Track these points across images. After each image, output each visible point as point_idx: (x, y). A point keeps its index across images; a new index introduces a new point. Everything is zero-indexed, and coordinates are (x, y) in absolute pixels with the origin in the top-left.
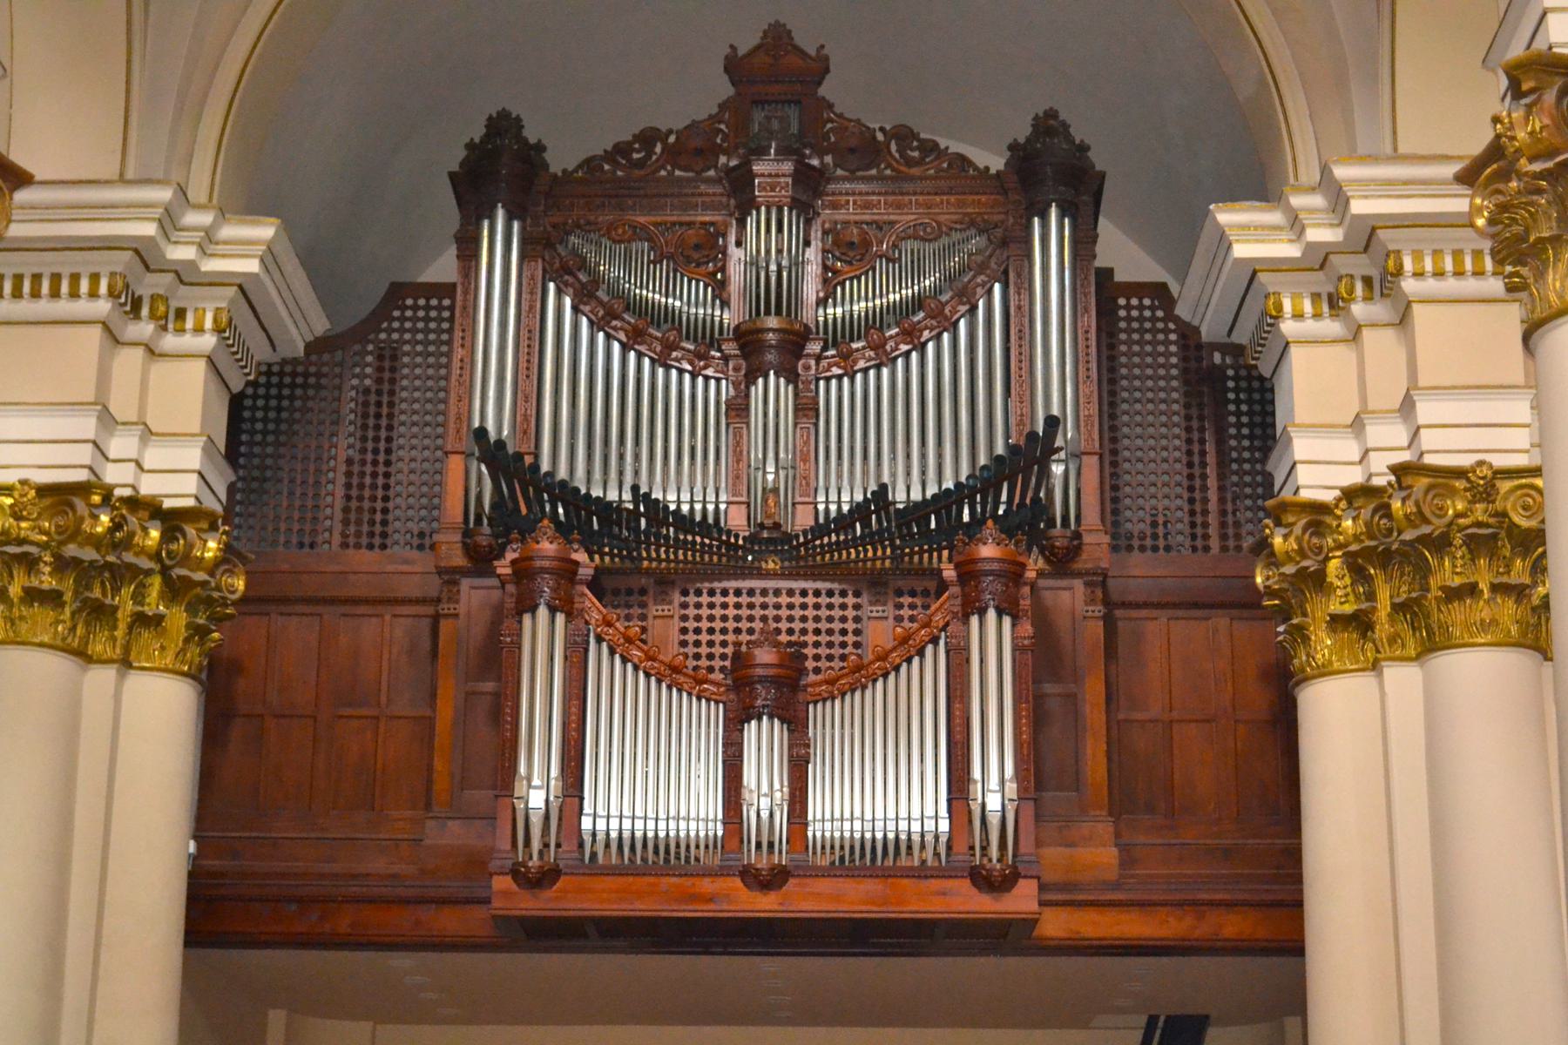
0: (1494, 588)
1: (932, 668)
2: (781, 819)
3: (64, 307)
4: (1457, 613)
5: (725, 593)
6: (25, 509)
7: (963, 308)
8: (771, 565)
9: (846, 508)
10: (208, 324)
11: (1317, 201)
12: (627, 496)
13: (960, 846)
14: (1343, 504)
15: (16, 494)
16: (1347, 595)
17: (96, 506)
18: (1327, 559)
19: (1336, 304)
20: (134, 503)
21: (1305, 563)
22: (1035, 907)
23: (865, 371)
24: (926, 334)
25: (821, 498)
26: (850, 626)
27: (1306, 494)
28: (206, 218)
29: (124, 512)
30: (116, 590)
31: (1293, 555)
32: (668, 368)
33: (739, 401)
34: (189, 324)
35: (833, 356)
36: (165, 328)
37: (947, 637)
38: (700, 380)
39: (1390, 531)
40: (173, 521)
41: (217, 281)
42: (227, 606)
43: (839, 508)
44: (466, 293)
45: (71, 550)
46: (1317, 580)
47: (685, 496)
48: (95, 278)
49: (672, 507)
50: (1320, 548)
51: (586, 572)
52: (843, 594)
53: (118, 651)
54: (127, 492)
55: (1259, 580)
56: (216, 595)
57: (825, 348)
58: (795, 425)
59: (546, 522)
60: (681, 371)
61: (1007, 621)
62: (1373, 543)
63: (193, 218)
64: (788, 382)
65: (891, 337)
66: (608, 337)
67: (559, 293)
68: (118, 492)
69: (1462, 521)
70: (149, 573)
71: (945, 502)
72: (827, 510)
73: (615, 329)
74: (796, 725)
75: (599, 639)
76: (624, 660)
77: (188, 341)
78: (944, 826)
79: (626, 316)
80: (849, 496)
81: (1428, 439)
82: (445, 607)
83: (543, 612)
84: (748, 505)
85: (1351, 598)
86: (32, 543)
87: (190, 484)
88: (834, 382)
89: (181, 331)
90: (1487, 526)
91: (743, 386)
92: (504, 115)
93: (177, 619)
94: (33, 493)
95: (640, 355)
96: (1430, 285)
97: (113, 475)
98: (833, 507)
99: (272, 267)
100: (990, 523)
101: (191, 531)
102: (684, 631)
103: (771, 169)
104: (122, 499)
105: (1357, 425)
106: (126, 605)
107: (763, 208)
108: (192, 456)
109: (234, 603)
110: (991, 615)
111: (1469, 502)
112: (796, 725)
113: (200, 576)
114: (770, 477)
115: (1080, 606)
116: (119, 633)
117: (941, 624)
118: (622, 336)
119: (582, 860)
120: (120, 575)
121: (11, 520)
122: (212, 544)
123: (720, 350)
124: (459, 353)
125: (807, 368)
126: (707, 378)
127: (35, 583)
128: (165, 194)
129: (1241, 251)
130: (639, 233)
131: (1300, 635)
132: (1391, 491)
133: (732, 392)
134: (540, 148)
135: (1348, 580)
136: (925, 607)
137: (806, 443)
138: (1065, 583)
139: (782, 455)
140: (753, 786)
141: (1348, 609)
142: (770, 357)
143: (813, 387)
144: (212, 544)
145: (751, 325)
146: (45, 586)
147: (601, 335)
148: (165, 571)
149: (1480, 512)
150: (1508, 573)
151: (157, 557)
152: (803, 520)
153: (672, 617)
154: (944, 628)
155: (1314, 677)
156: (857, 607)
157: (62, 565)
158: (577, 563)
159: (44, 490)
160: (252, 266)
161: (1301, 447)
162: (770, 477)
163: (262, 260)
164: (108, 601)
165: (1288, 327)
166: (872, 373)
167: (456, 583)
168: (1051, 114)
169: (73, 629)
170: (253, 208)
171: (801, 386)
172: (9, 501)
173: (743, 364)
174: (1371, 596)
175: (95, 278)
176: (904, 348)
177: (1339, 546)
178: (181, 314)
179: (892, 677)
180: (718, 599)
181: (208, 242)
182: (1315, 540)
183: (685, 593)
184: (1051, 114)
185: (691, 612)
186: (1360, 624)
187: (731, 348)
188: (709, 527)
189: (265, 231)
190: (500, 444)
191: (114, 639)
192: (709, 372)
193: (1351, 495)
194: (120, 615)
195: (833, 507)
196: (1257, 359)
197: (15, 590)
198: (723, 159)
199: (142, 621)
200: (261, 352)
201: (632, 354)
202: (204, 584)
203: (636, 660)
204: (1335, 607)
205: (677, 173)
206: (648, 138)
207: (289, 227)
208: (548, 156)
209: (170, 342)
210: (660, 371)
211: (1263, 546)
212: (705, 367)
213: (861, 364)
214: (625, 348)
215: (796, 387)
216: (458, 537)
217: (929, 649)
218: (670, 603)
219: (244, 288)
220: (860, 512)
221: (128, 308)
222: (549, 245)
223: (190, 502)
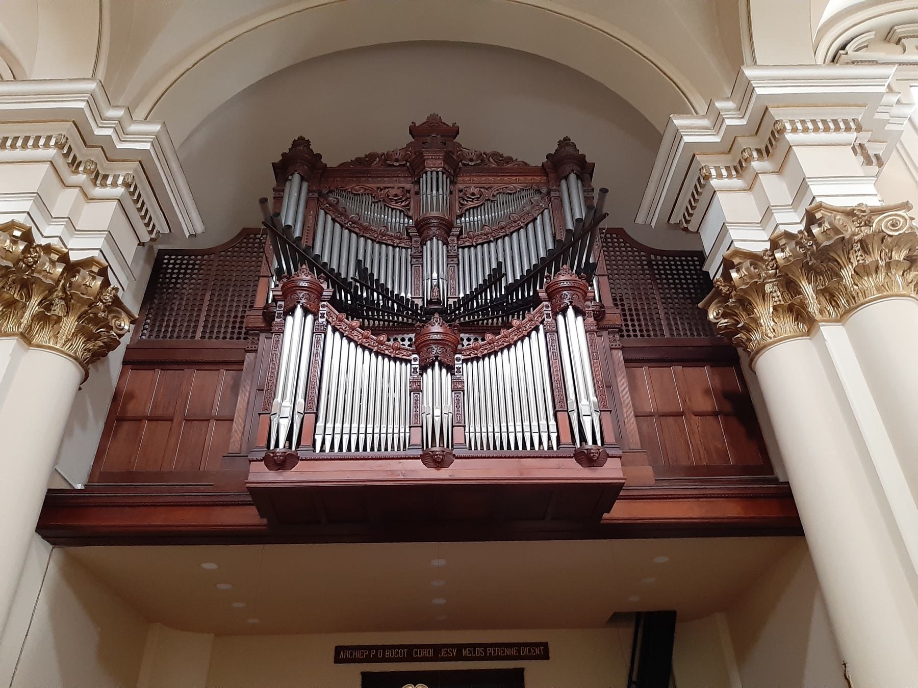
4: (869, 283)
11: (730, 105)
19: (739, 168)
30: (29, 297)
32: (380, 243)
34: (109, 181)
35: (466, 238)
41: (126, 156)
57: (461, 233)
67: (326, 213)
69: (856, 237)
77: (108, 191)
89: (104, 185)
92: (301, 138)
93: (69, 324)
96: (800, 137)
117: (540, 319)
119: (314, 451)
125: (453, 240)
129: (686, 139)
137: (454, 272)
142: (434, 230)
149: (866, 231)
155: (770, 344)
158: (323, 289)
160: (148, 146)
165: (714, 182)
167: (258, 335)
168: (567, 139)
171: (449, 248)
173: (420, 240)
177: (770, 277)
178: (106, 177)
184: (567, 139)
192: (403, 245)
203: (356, 338)
209: (98, 191)
215: (447, 247)
219: (143, 162)
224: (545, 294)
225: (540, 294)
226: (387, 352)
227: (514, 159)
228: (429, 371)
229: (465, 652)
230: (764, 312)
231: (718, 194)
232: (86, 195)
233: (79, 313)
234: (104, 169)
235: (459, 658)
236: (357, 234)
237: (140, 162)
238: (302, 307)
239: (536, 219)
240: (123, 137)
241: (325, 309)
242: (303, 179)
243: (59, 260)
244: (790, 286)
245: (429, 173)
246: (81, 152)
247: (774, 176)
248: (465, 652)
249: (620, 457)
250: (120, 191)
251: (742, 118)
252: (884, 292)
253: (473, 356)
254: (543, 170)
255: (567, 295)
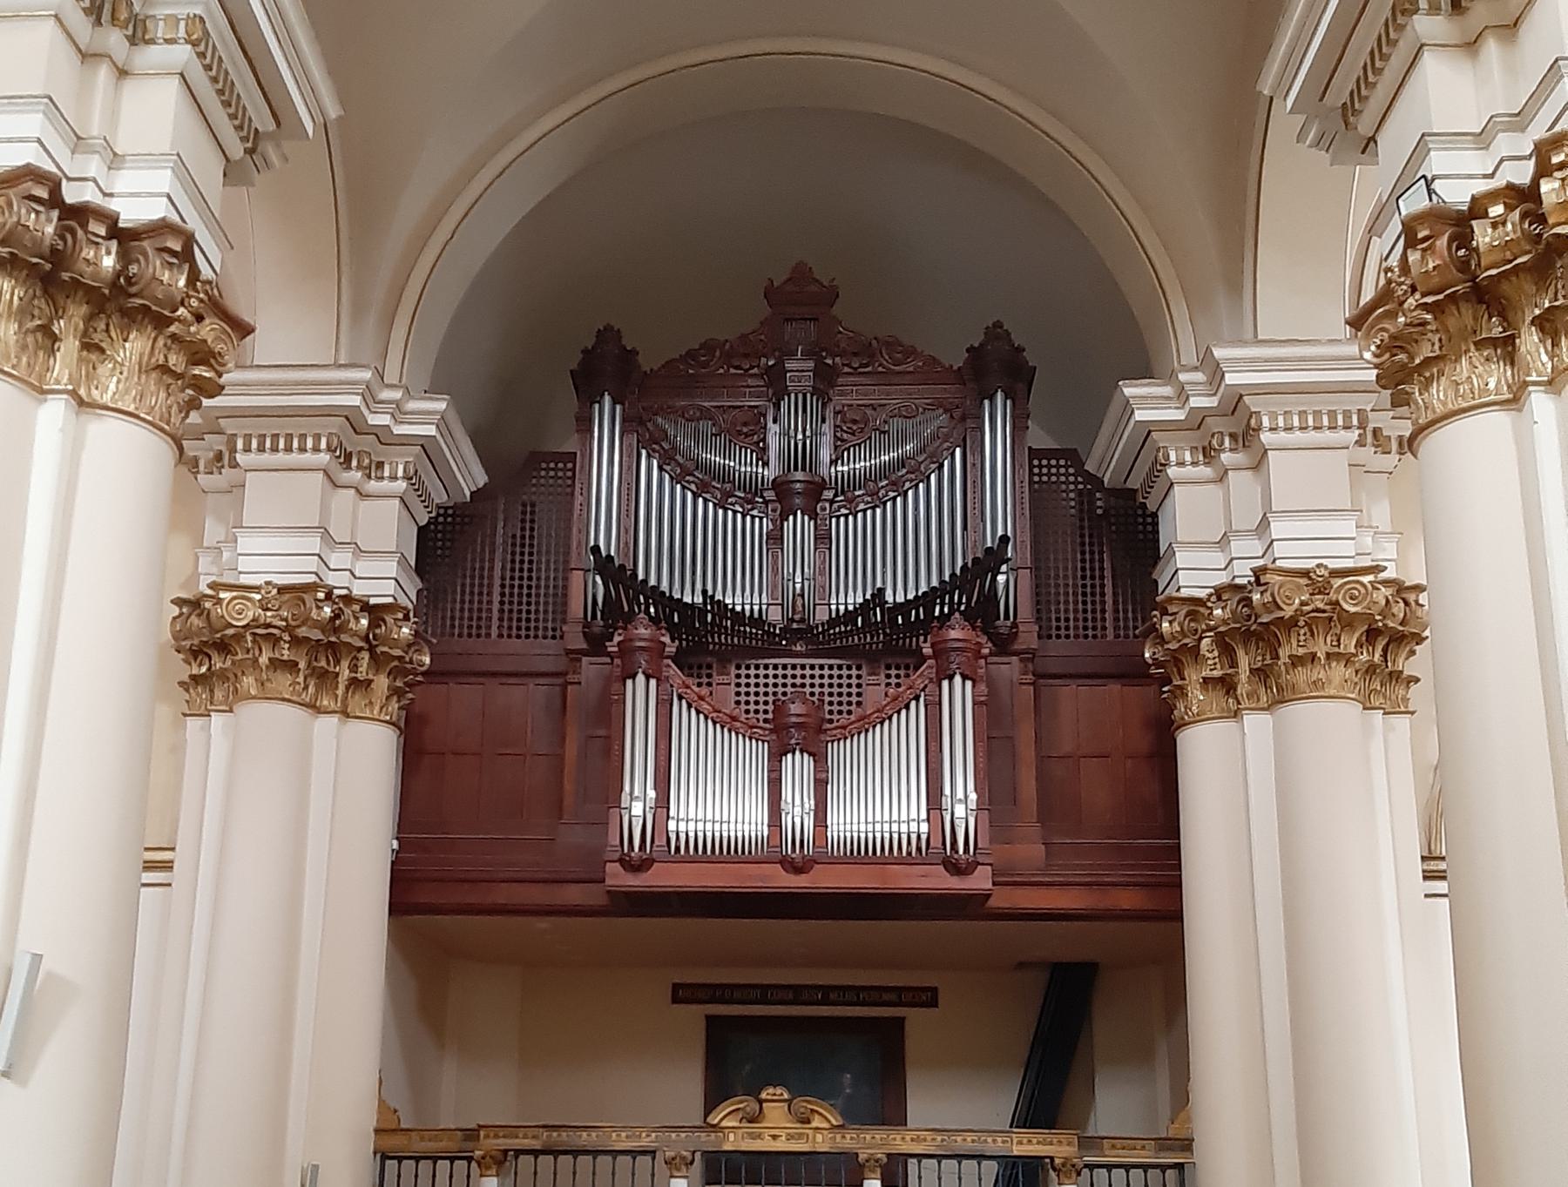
0: (1328, 655)
1: (916, 716)
2: (809, 823)
3: (295, 458)
4: (1302, 676)
5: (766, 667)
6: (269, 602)
7: (933, 466)
8: (799, 648)
9: (851, 608)
10: (400, 473)
12: (699, 599)
13: (936, 842)
14: (1213, 598)
15: (263, 592)
16: (1215, 664)
17: (320, 601)
18: (1201, 638)
19: (1208, 454)
20: (348, 599)
21: (1186, 641)
22: (990, 886)
23: (864, 511)
24: (907, 485)
25: (833, 601)
26: (854, 690)
27: (1184, 593)
28: (397, 395)
29: (341, 605)
30: (338, 662)
31: (1176, 635)
32: (726, 510)
33: (775, 532)
35: (841, 501)
36: (369, 477)
37: (925, 695)
38: (748, 518)
39: (1249, 616)
40: (376, 613)
41: (406, 440)
42: (416, 675)
43: (846, 608)
44: (583, 456)
45: (303, 632)
46: (1195, 651)
47: (738, 600)
48: (317, 437)
49: (730, 607)
50: (1196, 630)
51: (671, 649)
52: (849, 668)
53: (339, 704)
54: (344, 592)
55: (1147, 655)
56: (409, 666)
57: (836, 495)
58: (816, 549)
59: (642, 615)
60: (735, 512)
61: (969, 684)
62: (1238, 625)
63: (386, 394)
64: (810, 519)
65: (883, 487)
66: (684, 488)
67: (649, 456)
68: (337, 592)
70: (360, 649)
71: (926, 600)
72: (838, 610)
73: (688, 482)
74: (820, 758)
75: (680, 698)
76: (698, 712)
77: (385, 485)
78: (924, 827)
79: (696, 473)
80: (855, 599)
81: (1279, 549)
82: (570, 678)
83: (641, 678)
84: (782, 605)
85: (1218, 666)
86: (275, 627)
87: (390, 587)
88: (842, 519)
90: (1324, 611)
91: (778, 522)
92: (608, 328)
94: (275, 591)
95: (706, 501)
97: (331, 579)
98: (842, 608)
99: (445, 432)
100: (957, 615)
101: (389, 619)
102: (738, 694)
103: (799, 368)
104: (339, 597)
105: (1223, 543)
106: (345, 674)
107: (793, 396)
108: (391, 568)
109: (423, 674)
110: (958, 679)
111: (1311, 594)
112: (820, 758)
113: (397, 652)
114: (798, 586)
115: (1016, 676)
116: (340, 692)
117: (922, 686)
118: (693, 487)
119: (670, 851)
120: (335, 650)
121: (260, 611)
122: (405, 630)
123: (762, 497)
124: (579, 499)
125: (824, 509)
126: (753, 517)
127: (277, 655)
128: (367, 375)
130: (705, 414)
131: (1181, 691)
132: (1250, 587)
133: (771, 527)
134: (634, 352)
135: (1216, 653)
136: (907, 676)
138: (1005, 659)
139: (806, 570)
140: (789, 800)
141: (1217, 673)
143: (828, 522)
144: (405, 630)
145: (784, 478)
146: (285, 658)
147: (679, 486)
148: (371, 649)
150: (1339, 646)
151: (366, 639)
152: (822, 615)
153: (729, 684)
154: (923, 690)
156: (859, 677)
157: (296, 642)
159: (282, 590)
160: (431, 430)
161: (1182, 558)
162: (798, 586)
163: (438, 426)
164: (332, 669)
165: (1173, 472)
166: (869, 512)
167: (580, 660)
168: (998, 325)
169: (306, 688)
170: (433, 390)
171: (819, 522)
172: (258, 597)
174: (1234, 664)
175: (317, 437)
176: (892, 494)
178: (380, 465)
179: (886, 723)
180: (762, 672)
181: (398, 412)
182: (1192, 624)
183: (738, 667)
185: (743, 681)
186: (1227, 685)
187: (770, 495)
188: (758, 621)
189: (441, 406)
190: (609, 556)
191: (337, 696)
192: (755, 512)
193: (1219, 592)
194: (340, 679)
195: (842, 608)
196: (1146, 498)
197: (263, 660)
198: (763, 360)
199: (354, 683)
200: (440, 497)
201: (701, 500)
202: (400, 658)
203: (706, 712)
204: (1206, 673)
205: (732, 371)
206: (709, 347)
207: (457, 403)
208: (640, 358)
209: (373, 486)
210: (720, 512)
211: (1154, 630)
212: (752, 509)
213: (862, 506)
214: (695, 496)
215: (816, 523)
216: (580, 628)
217: (913, 704)
218: (728, 674)
219: (426, 447)
220: (865, 608)
221: (342, 460)
222: (642, 423)
223: (390, 600)
224: (930, 650)
225: (924, 650)
226: (741, 731)
227: (919, 350)
228: (789, 756)
229: (832, 996)
230: (1193, 676)
231: (1176, 488)
232: (361, 494)
233: (388, 670)
234: (377, 454)
235: (825, 1002)
236: (692, 491)
237: (422, 446)
238: (644, 673)
239: (892, 715)
240: (400, 417)
241: (673, 671)
242: (614, 402)
243: (362, 610)
244: (1227, 651)
245: (793, 396)
246: (354, 443)
247: (1249, 473)
248: (832, 996)
249: (991, 865)
250: (401, 485)
251: (1215, 394)
252: (1317, 691)
253: (839, 736)
254: (958, 376)
255: (956, 659)
